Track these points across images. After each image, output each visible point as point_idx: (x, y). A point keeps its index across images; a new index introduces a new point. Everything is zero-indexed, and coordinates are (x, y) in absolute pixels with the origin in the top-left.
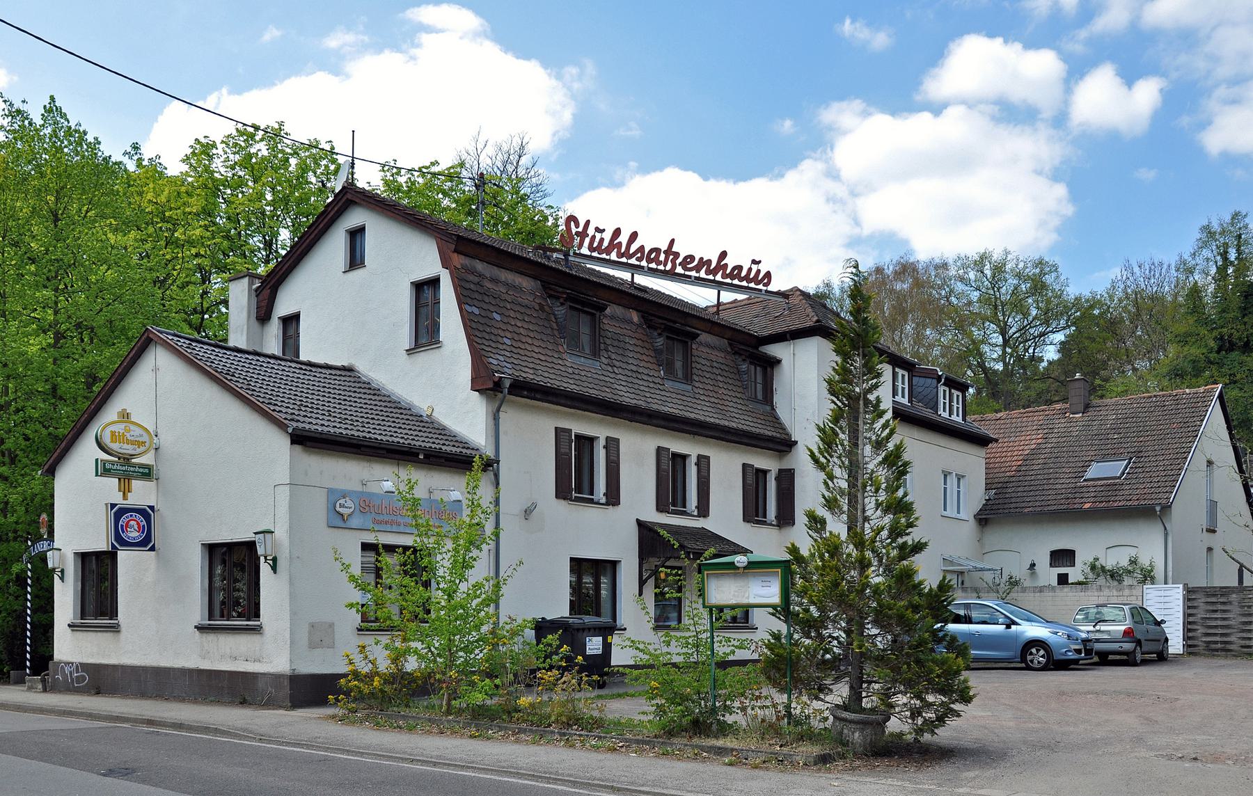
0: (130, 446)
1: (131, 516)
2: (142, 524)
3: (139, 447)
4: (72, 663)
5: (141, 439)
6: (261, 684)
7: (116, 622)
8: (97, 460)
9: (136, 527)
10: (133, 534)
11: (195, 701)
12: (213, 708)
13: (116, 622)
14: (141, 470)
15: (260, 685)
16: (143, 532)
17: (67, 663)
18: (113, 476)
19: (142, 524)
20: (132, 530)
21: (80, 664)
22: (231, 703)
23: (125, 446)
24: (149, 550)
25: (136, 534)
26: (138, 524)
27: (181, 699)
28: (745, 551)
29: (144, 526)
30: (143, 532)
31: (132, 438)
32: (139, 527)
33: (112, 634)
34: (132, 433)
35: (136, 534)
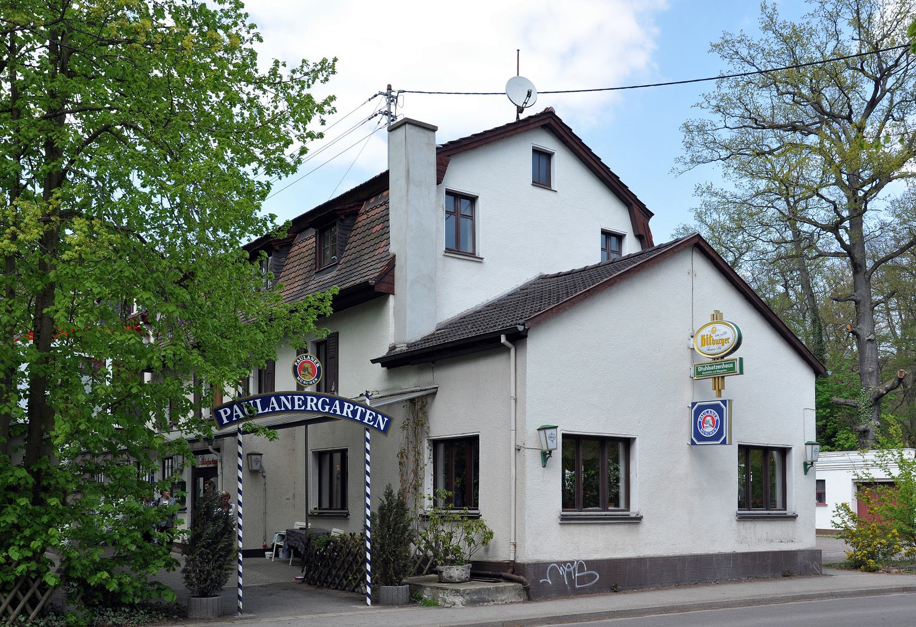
0: (716, 346)
1: (707, 412)
2: (716, 419)
3: (723, 345)
4: (572, 563)
5: (724, 337)
6: (800, 559)
7: (346, 511)
8: (741, 372)
9: (711, 422)
10: (709, 430)
11: (739, 581)
12: (543, 603)
13: (346, 511)
14: (727, 366)
15: (799, 560)
16: (716, 427)
17: (560, 564)
18: (707, 377)
19: (716, 419)
20: (306, 373)
21: (586, 562)
22: (775, 578)
23: (712, 347)
24: (722, 443)
25: (710, 429)
26: (713, 419)
27: (718, 582)
28: (313, 83)
29: (319, 367)
30: (716, 427)
31: (717, 338)
32: (713, 422)
33: (627, 526)
34: (717, 333)
35: (710, 429)
